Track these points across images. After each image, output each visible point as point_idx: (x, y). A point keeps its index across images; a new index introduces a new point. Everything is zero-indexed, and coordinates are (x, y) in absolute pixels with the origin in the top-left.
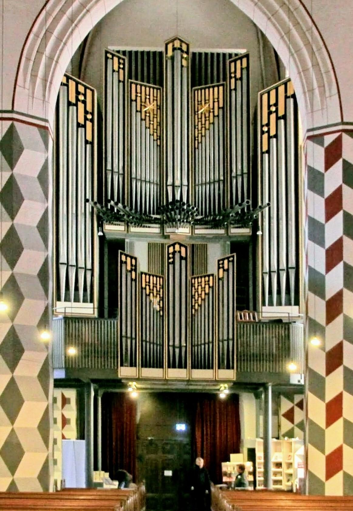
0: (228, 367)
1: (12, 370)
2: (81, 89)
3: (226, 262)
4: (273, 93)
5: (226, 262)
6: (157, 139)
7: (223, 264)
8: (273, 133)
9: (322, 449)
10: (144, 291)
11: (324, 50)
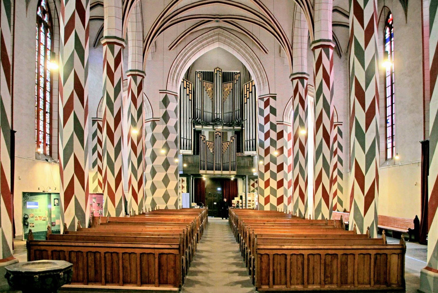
0: (234, 170)
2: (188, 83)
3: (233, 137)
4: (248, 85)
5: (233, 137)
8: (248, 97)
11: (264, 71)
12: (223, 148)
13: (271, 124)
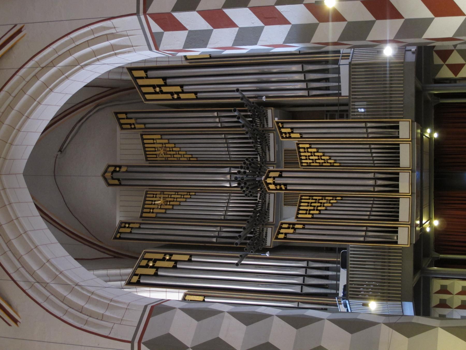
0: (397, 127)
2: (144, 263)
3: (283, 130)
4: (145, 90)
5: (283, 130)
6: (189, 195)
7: (285, 133)
10: (315, 216)
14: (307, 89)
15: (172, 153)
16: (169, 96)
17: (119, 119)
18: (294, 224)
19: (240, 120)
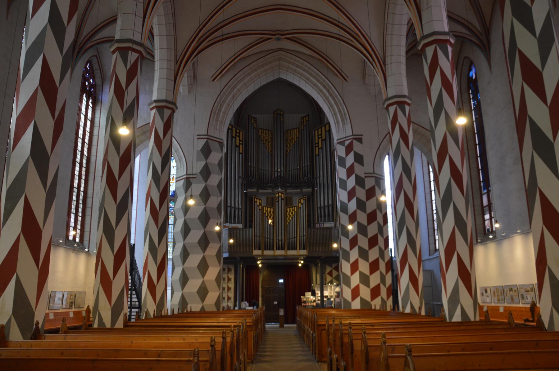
0: (304, 249)
1: (204, 252)
2: (238, 131)
3: (302, 200)
5: (302, 200)
7: (301, 201)
9: (349, 286)
10: (265, 214)
12: (287, 216)
13: (357, 177)
14: (321, 207)
15: (290, 143)
16: (317, 142)
17: (306, 117)
18: (261, 205)
19: (306, 178)
